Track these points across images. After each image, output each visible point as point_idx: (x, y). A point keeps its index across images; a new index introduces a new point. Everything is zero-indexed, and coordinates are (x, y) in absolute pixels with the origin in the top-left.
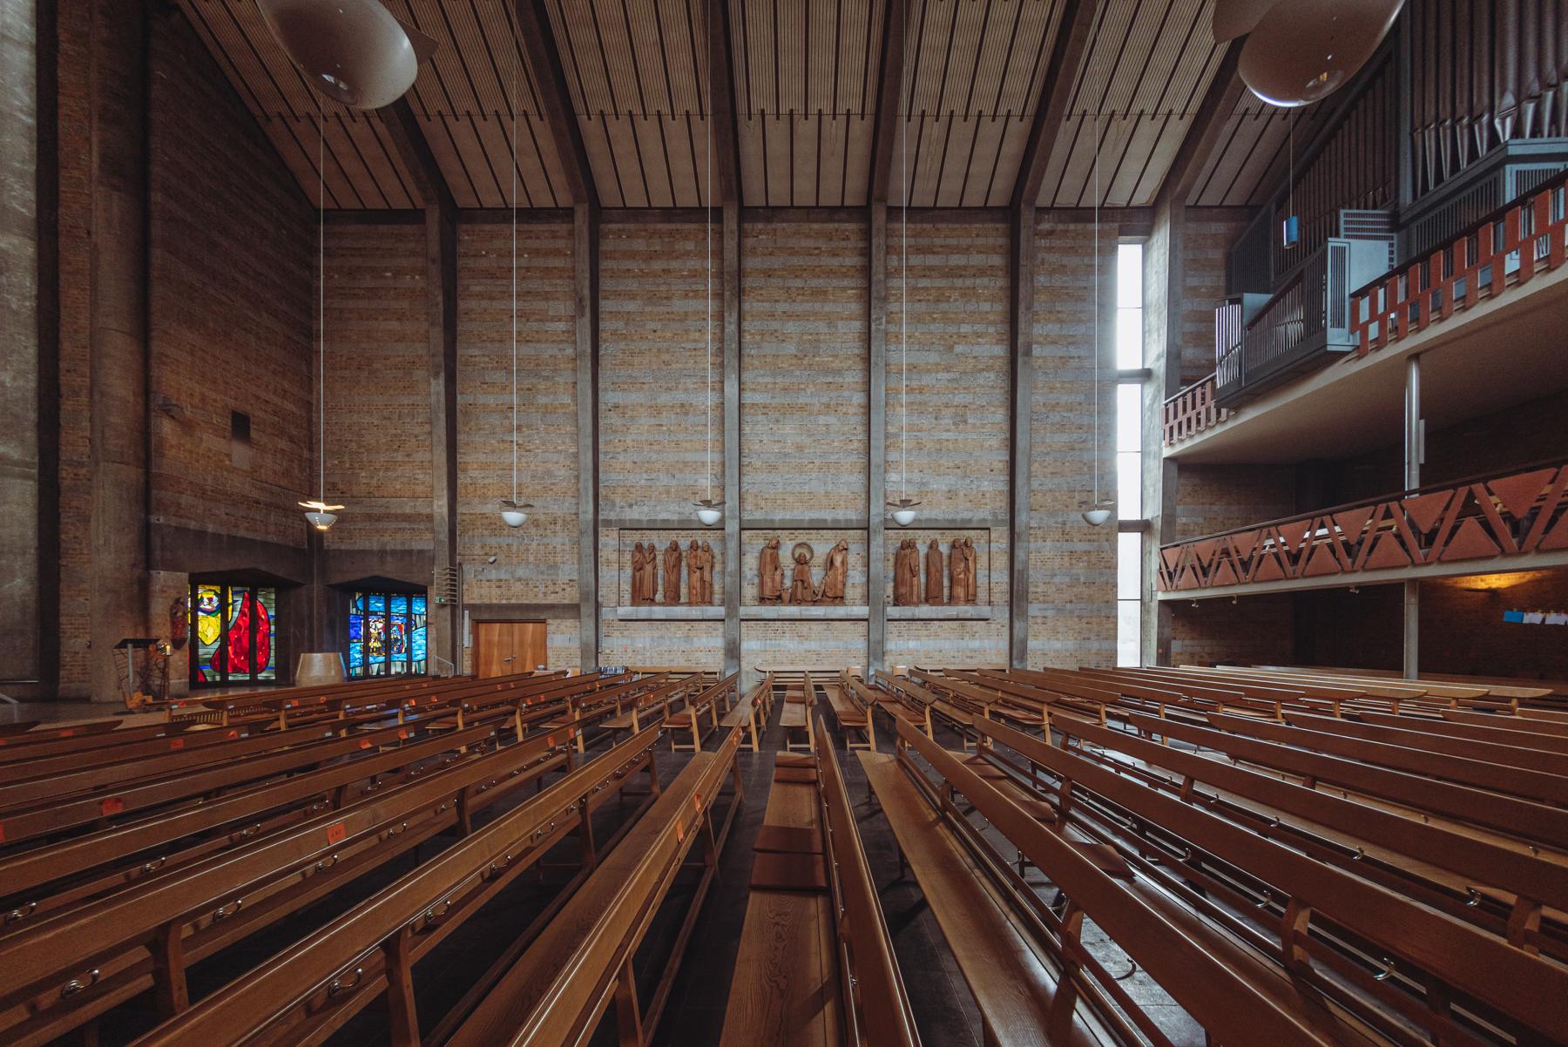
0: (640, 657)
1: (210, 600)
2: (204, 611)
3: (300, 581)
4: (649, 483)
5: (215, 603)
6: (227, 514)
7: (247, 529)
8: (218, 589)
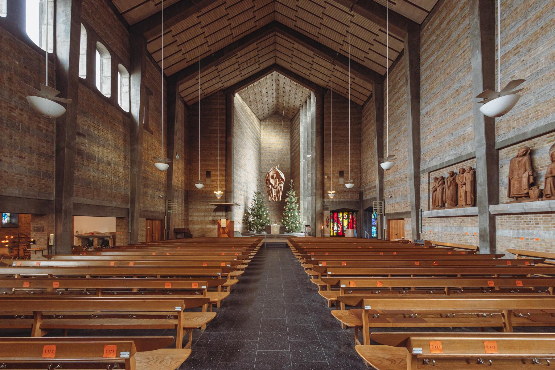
0: (437, 237)
2: (345, 219)
3: (357, 210)
4: (441, 144)
5: (347, 217)
8: (347, 213)
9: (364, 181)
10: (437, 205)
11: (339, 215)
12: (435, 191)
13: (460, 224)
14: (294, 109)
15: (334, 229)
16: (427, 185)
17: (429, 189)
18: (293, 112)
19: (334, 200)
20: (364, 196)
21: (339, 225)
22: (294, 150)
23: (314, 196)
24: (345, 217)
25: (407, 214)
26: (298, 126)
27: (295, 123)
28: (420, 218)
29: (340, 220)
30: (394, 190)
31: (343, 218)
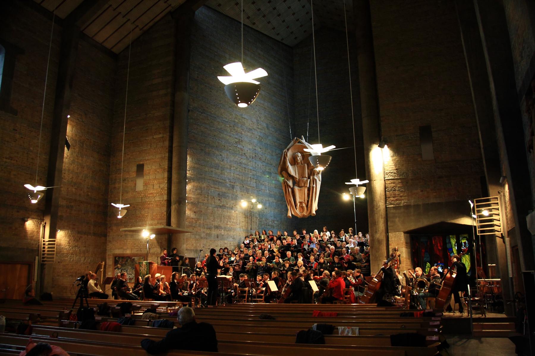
1: (465, 243)
6: (422, 191)
31: (459, 250)
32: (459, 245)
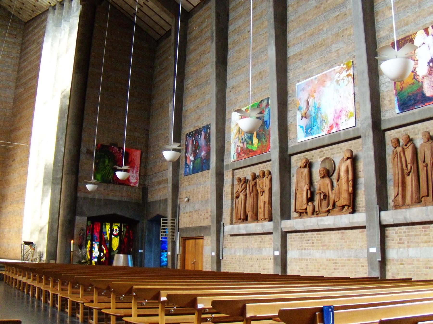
1: (116, 230)
5: (118, 232)
7: (113, 195)
8: (119, 225)
9: (151, 168)
10: (239, 218)
11: (104, 227)
12: (238, 197)
13: (260, 244)
14: (35, 6)
15: (94, 255)
16: (231, 187)
17: (232, 194)
18: (33, 11)
19: (97, 196)
20: (149, 195)
21: (103, 246)
22: (25, 83)
23: (58, 184)
24: (115, 233)
25: (205, 228)
26: (39, 38)
27: (33, 31)
28: (221, 235)
29: (105, 237)
30: (192, 190)
31: (111, 234)
32: (112, 230)
